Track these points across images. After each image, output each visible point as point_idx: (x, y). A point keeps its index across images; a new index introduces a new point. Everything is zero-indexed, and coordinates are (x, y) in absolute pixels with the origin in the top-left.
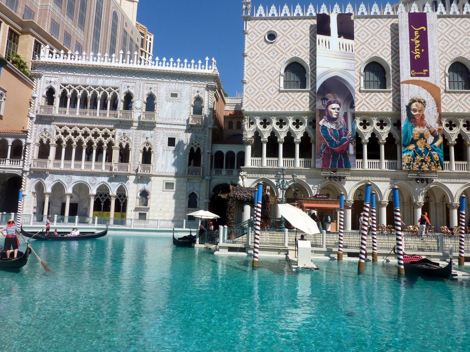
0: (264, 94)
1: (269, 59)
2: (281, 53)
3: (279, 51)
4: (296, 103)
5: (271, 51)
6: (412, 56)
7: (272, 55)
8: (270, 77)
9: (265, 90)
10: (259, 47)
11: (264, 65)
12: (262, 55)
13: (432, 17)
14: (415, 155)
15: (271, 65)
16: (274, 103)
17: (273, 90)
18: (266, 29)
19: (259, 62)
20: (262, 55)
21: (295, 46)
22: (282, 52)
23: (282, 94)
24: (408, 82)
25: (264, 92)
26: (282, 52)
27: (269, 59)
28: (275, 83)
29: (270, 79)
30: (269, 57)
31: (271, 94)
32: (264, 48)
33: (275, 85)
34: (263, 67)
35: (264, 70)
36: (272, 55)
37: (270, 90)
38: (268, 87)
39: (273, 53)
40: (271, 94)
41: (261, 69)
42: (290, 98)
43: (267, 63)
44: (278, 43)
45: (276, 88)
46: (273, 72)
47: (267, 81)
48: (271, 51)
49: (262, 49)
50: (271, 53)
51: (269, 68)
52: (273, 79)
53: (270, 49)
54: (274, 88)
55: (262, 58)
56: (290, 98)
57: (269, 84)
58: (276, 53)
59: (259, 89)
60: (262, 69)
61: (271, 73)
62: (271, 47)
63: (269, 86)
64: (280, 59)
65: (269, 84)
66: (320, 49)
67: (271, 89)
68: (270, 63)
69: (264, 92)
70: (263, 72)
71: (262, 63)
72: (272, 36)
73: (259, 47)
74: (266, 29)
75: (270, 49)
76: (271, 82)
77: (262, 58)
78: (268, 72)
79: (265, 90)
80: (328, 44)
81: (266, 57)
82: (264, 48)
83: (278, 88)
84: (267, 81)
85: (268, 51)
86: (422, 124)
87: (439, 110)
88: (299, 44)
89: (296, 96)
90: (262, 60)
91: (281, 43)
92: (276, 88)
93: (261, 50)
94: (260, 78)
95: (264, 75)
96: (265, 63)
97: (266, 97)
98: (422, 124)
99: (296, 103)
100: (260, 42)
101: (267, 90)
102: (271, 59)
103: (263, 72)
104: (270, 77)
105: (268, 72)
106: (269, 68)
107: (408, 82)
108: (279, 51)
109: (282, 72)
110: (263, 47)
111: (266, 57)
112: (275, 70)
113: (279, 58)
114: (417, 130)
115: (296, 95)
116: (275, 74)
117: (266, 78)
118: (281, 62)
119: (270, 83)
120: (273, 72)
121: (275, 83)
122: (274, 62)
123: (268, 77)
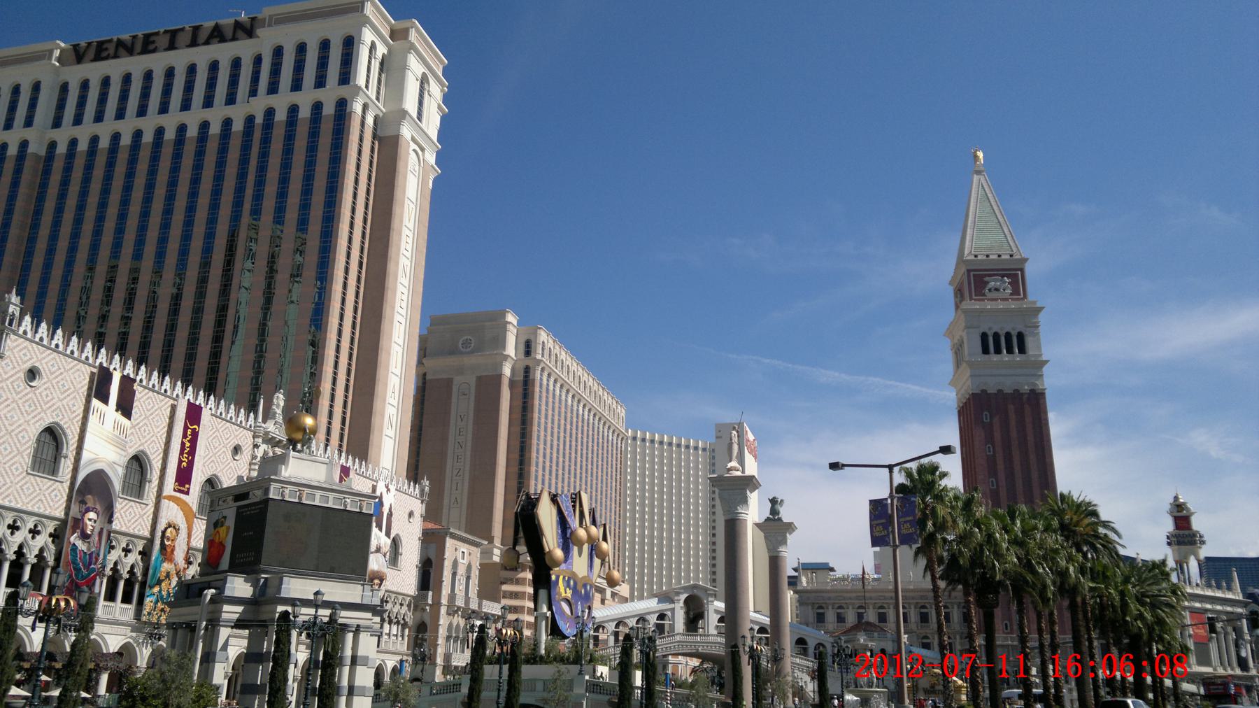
6: (180, 462)
13: (206, 415)
14: (157, 602)
21: (59, 404)
24: (170, 498)
49: (17, 393)
60: (10, 428)
66: (93, 420)
72: (32, 374)
80: (102, 418)
86: (171, 560)
87: (188, 543)
88: (64, 402)
98: (171, 560)
107: (170, 498)
114: (166, 566)
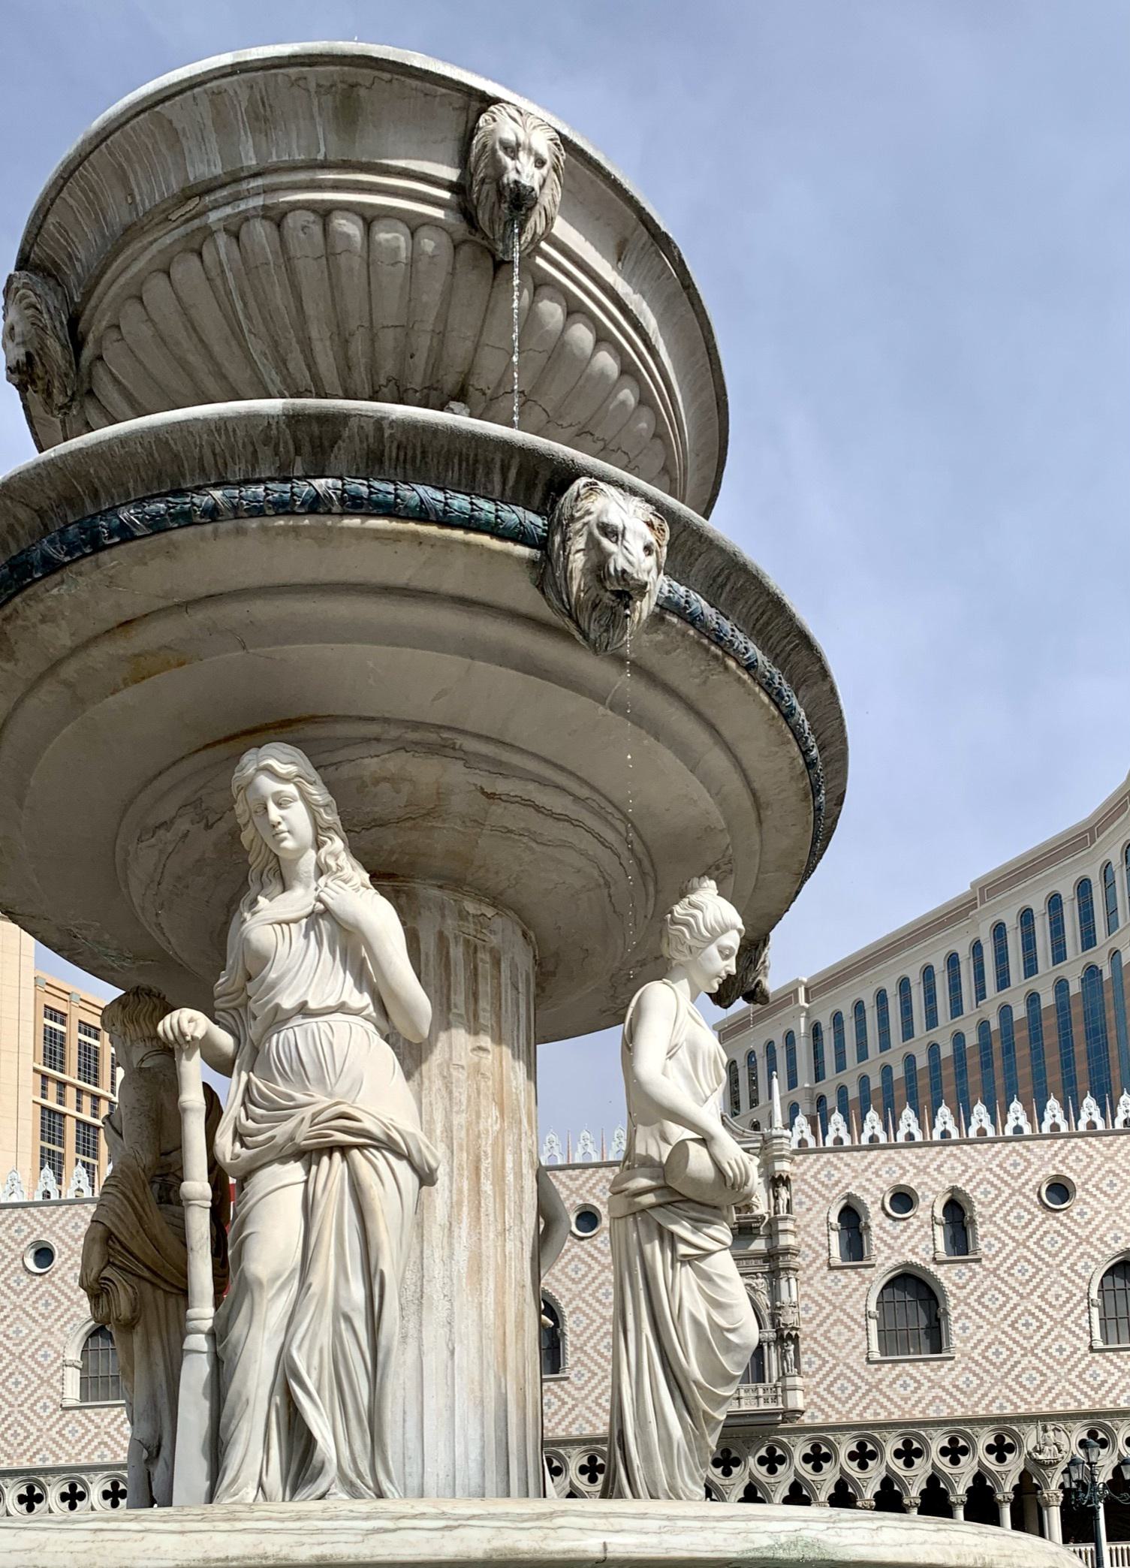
0: (22, 1419)
1: (35, 1321)
2: (67, 1303)
3: (62, 1298)
4: (106, 1439)
5: (40, 1298)
7: (42, 1309)
8: (39, 1371)
9: (25, 1408)
10: (9, 1287)
11: (23, 1340)
12: (18, 1312)
15: (39, 1336)
16: (50, 1443)
17: (45, 1407)
18: (26, 1237)
19: (10, 1332)
20: (18, 1312)
22: (69, 1299)
23: (69, 1415)
25: (21, 1412)
26: (69, 1299)
27: (35, 1321)
28: (52, 1387)
29: (39, 1377)
30: (34, 1314)
31: (40, 1417)
32: (22, 1291)
33: (50, 1391)
34: (20, 1344)
35: (24, 1351)
36: (42, 1309)
37: (37, 1408)
38: (32, 1401)
39: (47, 1304)
40: (40, 1417)
41: (13, 1349)
42: (91, 1427)
43: (31, 1331)
44: (59, 1274)
45: (54, 1401)
46: (45, 1356)
47: (31, 1382)
48: (40, 1298)
49: (18, 1294)
50: (40, 1305)
51: (36, 1345)
52: (45, 1377)
53: (38, 1293)
54: (49, 1403)
55: (18, 1318)
56: (91, 1427)
57: (35, 1391)
58: (54, 1304)
59: (11, 1405)
60: (17, 1350)
61: (41, 1359)
62: (40, 1285)
63: (36, 1396)
64: (65, 1319)
65: (35, 1391)
67: (40, 1404)
68: (38, 1331)
69: (21, 1412)
70: (20, 1358)
71: (18, 1332)
73: (9, 1287)
74: (26, 1237)
75: (38, 1293)
76: (41, 1385)
77: (18, 1318)
78: (32, 1356)
79: (25, 1408)
81: (28, 1315)
82: (22, 1291)
83: (59, 1400)
84: (31, 1382)
85: (33, 1298)
89: (107, 1421)
90: (18, 1324)
91: (65, 1275)
92: (54, 1401)
93: (13, 1297)
94: (11, 1374)
95: (22, 1368)
96: (25, 1331)
97: (29, 1427)
99: (106, 1439)
100: (13, 1273)
101: (31, 1408)
102: (41, 1321)
103: (20, 1358)
104: (39, 1371)
105: (32, 1356)
106: (36, 1345)
108: (62, 1298)
109: (74, 1354)
110: (18, 1288)
111: (28, 1315)
112: (51, 1352)
113: (62, 1316)
115: (107, 1414)
116: (53, 1362)
117: (28, 1373)
118: (67, 1329)
119: (39, 1387)
120: (45, 1356)
121: (52, 1387)
122: (49, 1330)
123: (33, 1371)
